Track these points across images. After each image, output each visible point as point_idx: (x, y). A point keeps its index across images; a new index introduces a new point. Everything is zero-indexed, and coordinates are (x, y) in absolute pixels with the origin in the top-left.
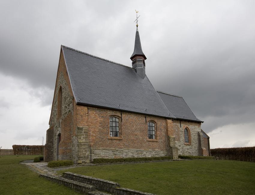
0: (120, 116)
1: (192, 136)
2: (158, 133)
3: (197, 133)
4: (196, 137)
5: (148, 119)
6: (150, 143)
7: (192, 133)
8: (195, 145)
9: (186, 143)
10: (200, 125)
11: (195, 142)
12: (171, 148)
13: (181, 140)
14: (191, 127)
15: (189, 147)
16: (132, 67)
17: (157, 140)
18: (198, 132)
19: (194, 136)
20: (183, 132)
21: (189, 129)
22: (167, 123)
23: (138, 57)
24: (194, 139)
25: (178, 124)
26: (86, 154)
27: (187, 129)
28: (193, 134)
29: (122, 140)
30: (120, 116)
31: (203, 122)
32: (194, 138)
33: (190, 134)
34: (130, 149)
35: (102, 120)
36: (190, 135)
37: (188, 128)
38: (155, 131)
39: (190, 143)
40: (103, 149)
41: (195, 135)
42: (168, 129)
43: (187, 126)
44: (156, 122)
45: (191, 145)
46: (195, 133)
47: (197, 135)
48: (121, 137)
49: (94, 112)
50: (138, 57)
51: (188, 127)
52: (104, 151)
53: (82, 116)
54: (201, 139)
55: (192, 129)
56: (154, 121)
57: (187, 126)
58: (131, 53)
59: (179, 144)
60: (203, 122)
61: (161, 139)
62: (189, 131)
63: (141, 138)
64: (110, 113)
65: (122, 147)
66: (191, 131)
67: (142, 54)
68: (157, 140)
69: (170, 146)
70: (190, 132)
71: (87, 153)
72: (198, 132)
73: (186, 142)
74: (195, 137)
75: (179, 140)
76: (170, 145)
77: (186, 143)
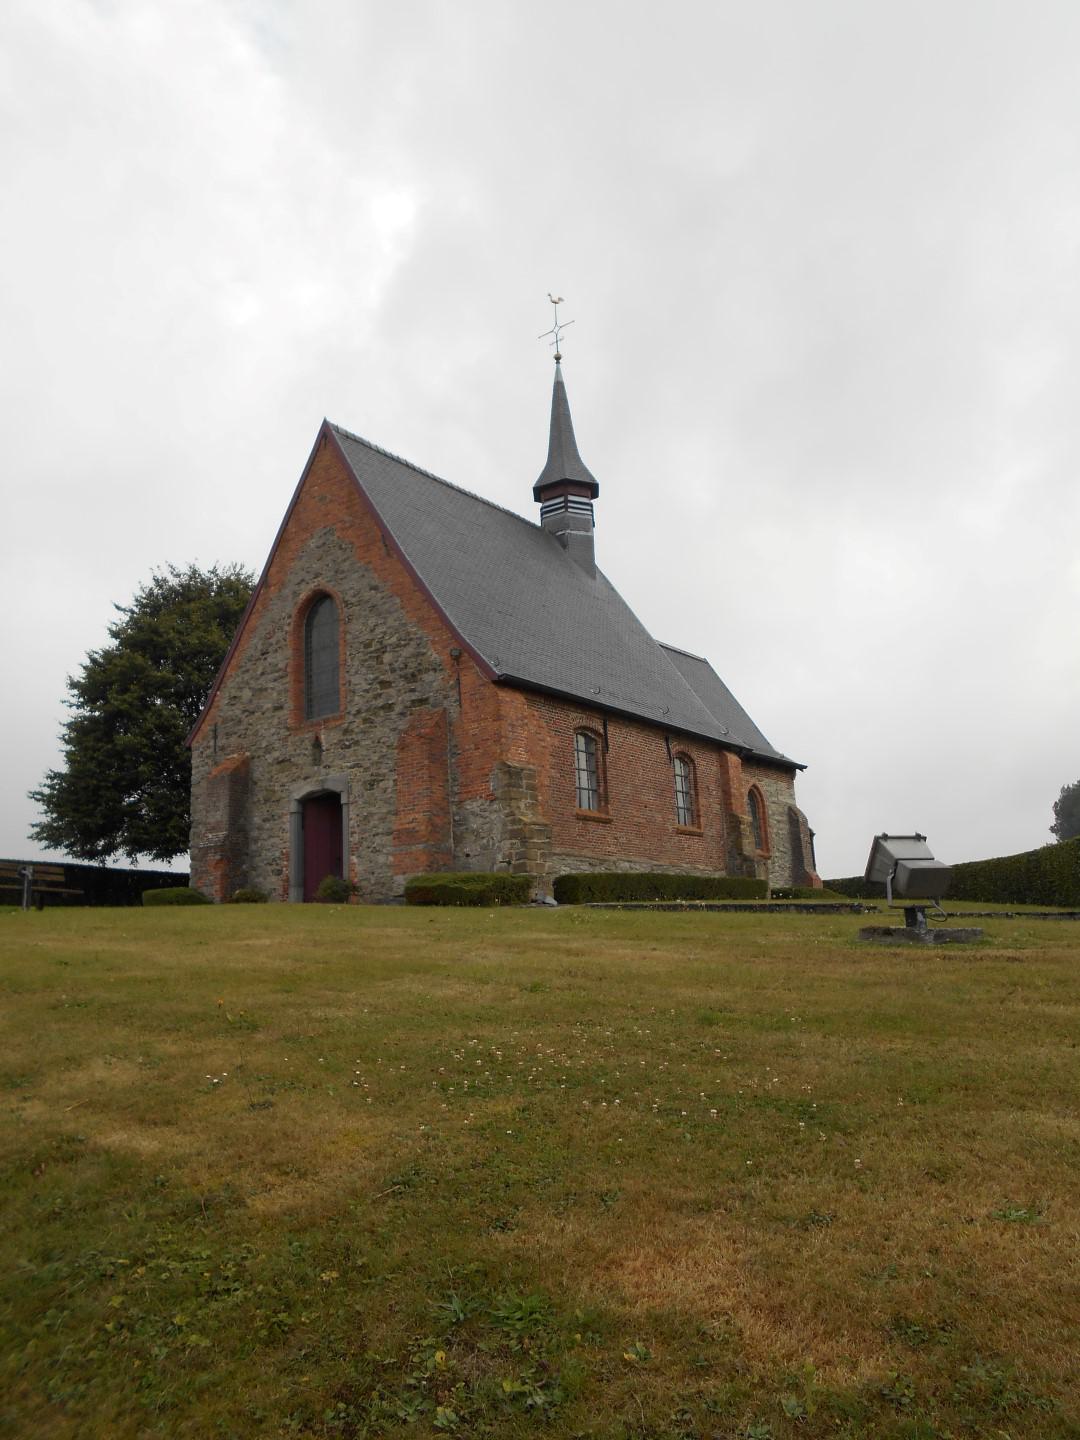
0: (602, 731)
1: (772, 821)
2: (702, 801)
3: (786, 809)
5: (675, 747)
6: (683, 838)
7: (770, 812)
10: (792, 776)
11: (781, 849)
12: (746, 859)
14: (768, 785)
16: (538, 523)
17: (699, 827)
19: (779, 822)
21: (761, 795)
22: (724, 768)
23: (566, 486)
24: (777, 834)
26: (543, 866)
27: (754, 795)
28: (774, 814)
29: (608, 822)
30: (602, 731)
31: (802, 768)
32: (778, 829)
33: (764, 812)
34: (633, 858)
35: (557, 743)
36: (764, 819)
38: (692, 792)
39: (768, 850)
40: (563, 854)
42: (730, 788)
43: (753, 781)
44: (692, 761)
46: (781, 810)
47: (785, 818)
48: (607, 813)
49: (536, 713)
50: (566, 486)
52: (569, 861)
53: (513, 726)
54: (802, 835)
56: (689, 757)
57: (753, 781)
58: (535, 462)
60: (802, 768)
61: (713, 826)
62: (762, 800)
63: (659, 818)
64: (577, 718)
65: (612, 849)
66: (767, 803)
67: (588, 480)
68: (699, 827)
69: (740, 854)
70: (764, 806)
71: (547, 864)
74: (782, 825)
76: (741, 850)
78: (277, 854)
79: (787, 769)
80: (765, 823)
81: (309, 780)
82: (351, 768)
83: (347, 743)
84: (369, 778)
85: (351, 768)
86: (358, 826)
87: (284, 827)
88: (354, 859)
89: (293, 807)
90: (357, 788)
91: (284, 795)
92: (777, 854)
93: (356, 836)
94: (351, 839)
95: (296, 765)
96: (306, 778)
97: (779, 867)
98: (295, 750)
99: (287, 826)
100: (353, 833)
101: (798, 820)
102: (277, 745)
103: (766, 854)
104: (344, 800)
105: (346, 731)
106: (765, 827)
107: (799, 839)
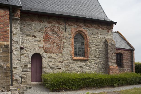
4: (101, 48)
8: (97, 60)
9: (76, 58)
10: (112, 28)
11: (98, 56)
13: (65, 51)
15: (84, 64)
18: (106, 40)
19: (97, 45)
20: (70, 38)
21: (85, 34)
25: (61, 27)
36: (87, 44)
37: (83, 32)
39: (87, 57)
41: (98, 44)
43: (80, 29)
45: (88, 60)
47: (102, 44)
51: (83, 30)
54: (109, 51)
55: (93, 34)
57: (80, 29)
59: (60, 59)
60: (115, 23)
62: (86, 37)
70: (87, 39)
72: (106, 40)
73: (76, 55)
74: (98, 47)
75: (59, 52)
77: (76, 58)
79: (110, 24)
80: (87, 46)
92: (94, 58)
97: (95, 63)
101: (107, 44)
103: (85, 59)
106: (87, 48)
107: (107, 52)
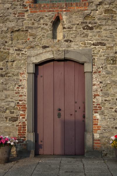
78: (13, 104)
81: (48, 49)
82: (93, 44)
83: (90, 25)
84: (112, 55)
85: (93, 44)
86: (101, 90)
87: (20, 83)
88: (97, 116)
89: (32, 69)
90: (99, 62)
91: (18, 57)
93: (99, 99)
94: (95, 100)
95: (34, 36)
96: (45, 47)
98: (33, 24)
99: (25, 83)
100: (95, 96)
102: (12, 17)
104: (87, 68)
105: (87, 16)
